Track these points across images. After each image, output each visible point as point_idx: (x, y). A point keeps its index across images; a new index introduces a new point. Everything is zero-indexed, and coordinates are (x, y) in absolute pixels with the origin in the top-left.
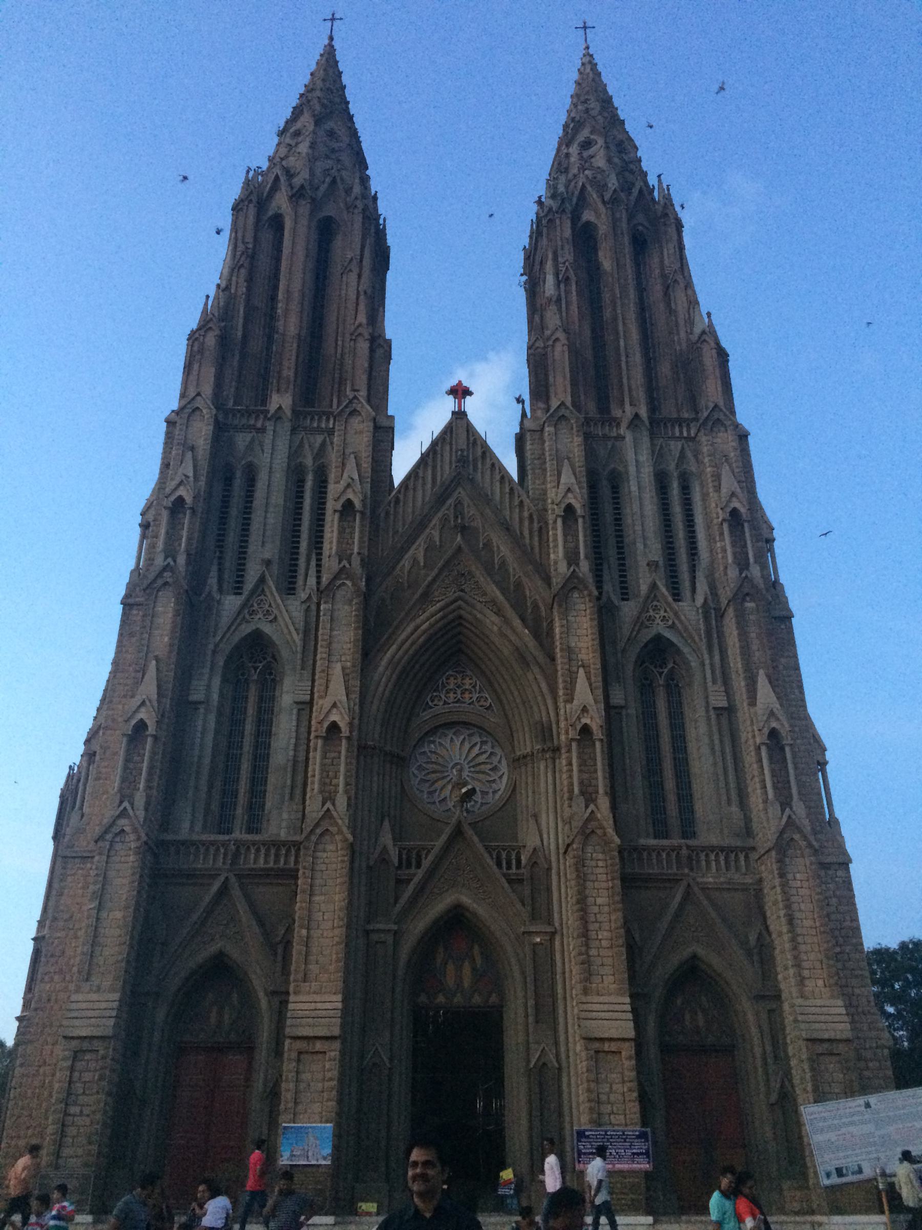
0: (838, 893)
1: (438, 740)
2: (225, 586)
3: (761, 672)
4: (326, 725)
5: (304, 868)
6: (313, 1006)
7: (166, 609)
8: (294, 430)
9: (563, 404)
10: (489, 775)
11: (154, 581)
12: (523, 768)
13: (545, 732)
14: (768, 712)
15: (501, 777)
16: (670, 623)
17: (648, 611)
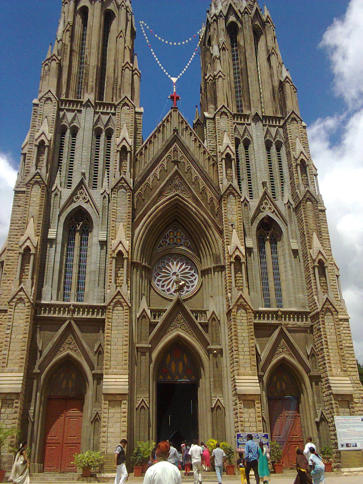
1: (165, 261)
2: (63, 184)
3: (314, 233)
4: (116, 252)
5: (108, 318)
6: (114, 380)
7: (36, 193)
8: (96, 113)
9: (224, 106)
10: (190, 278)
11: (31, 180)
12: (206, 276)
13: (217, 259)
14: (318, 251)
15: (195, 279)
16: (272, 210)
17: (262, 205)
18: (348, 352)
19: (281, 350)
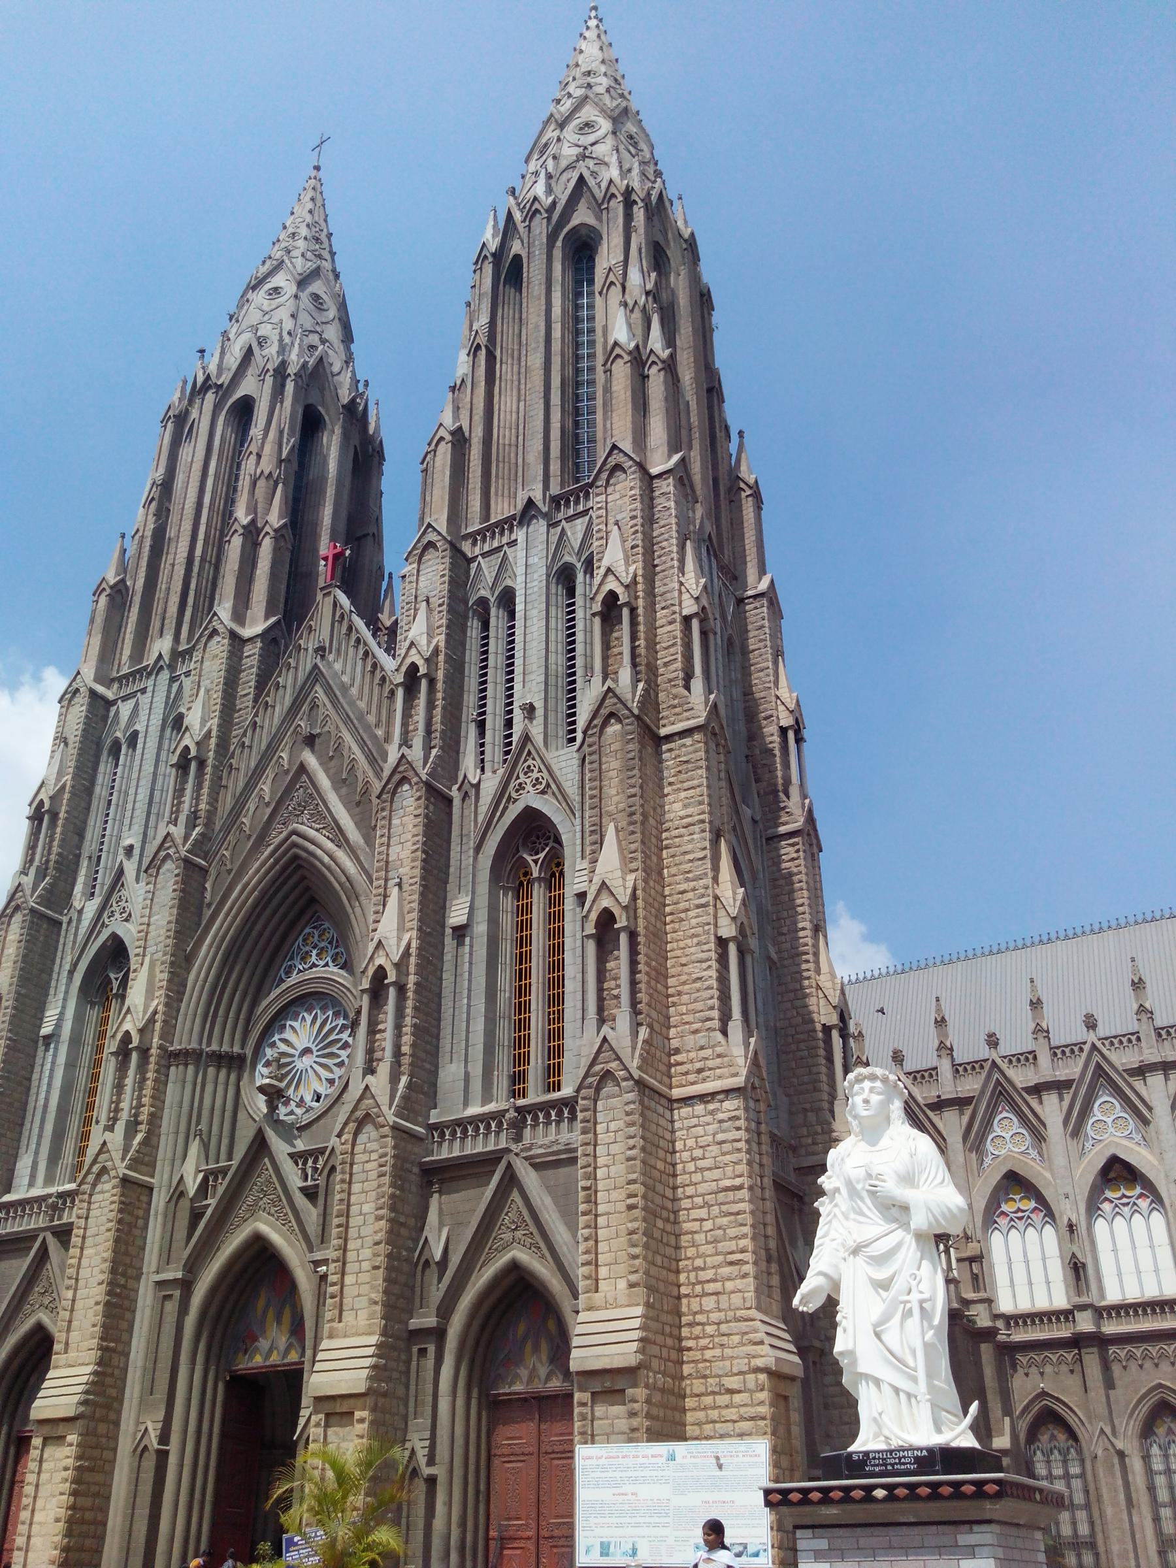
0: (720, 1137)
8: (173, 679)
16: (544, 783)
18: (724, 1208)
19: (508, 1236)
